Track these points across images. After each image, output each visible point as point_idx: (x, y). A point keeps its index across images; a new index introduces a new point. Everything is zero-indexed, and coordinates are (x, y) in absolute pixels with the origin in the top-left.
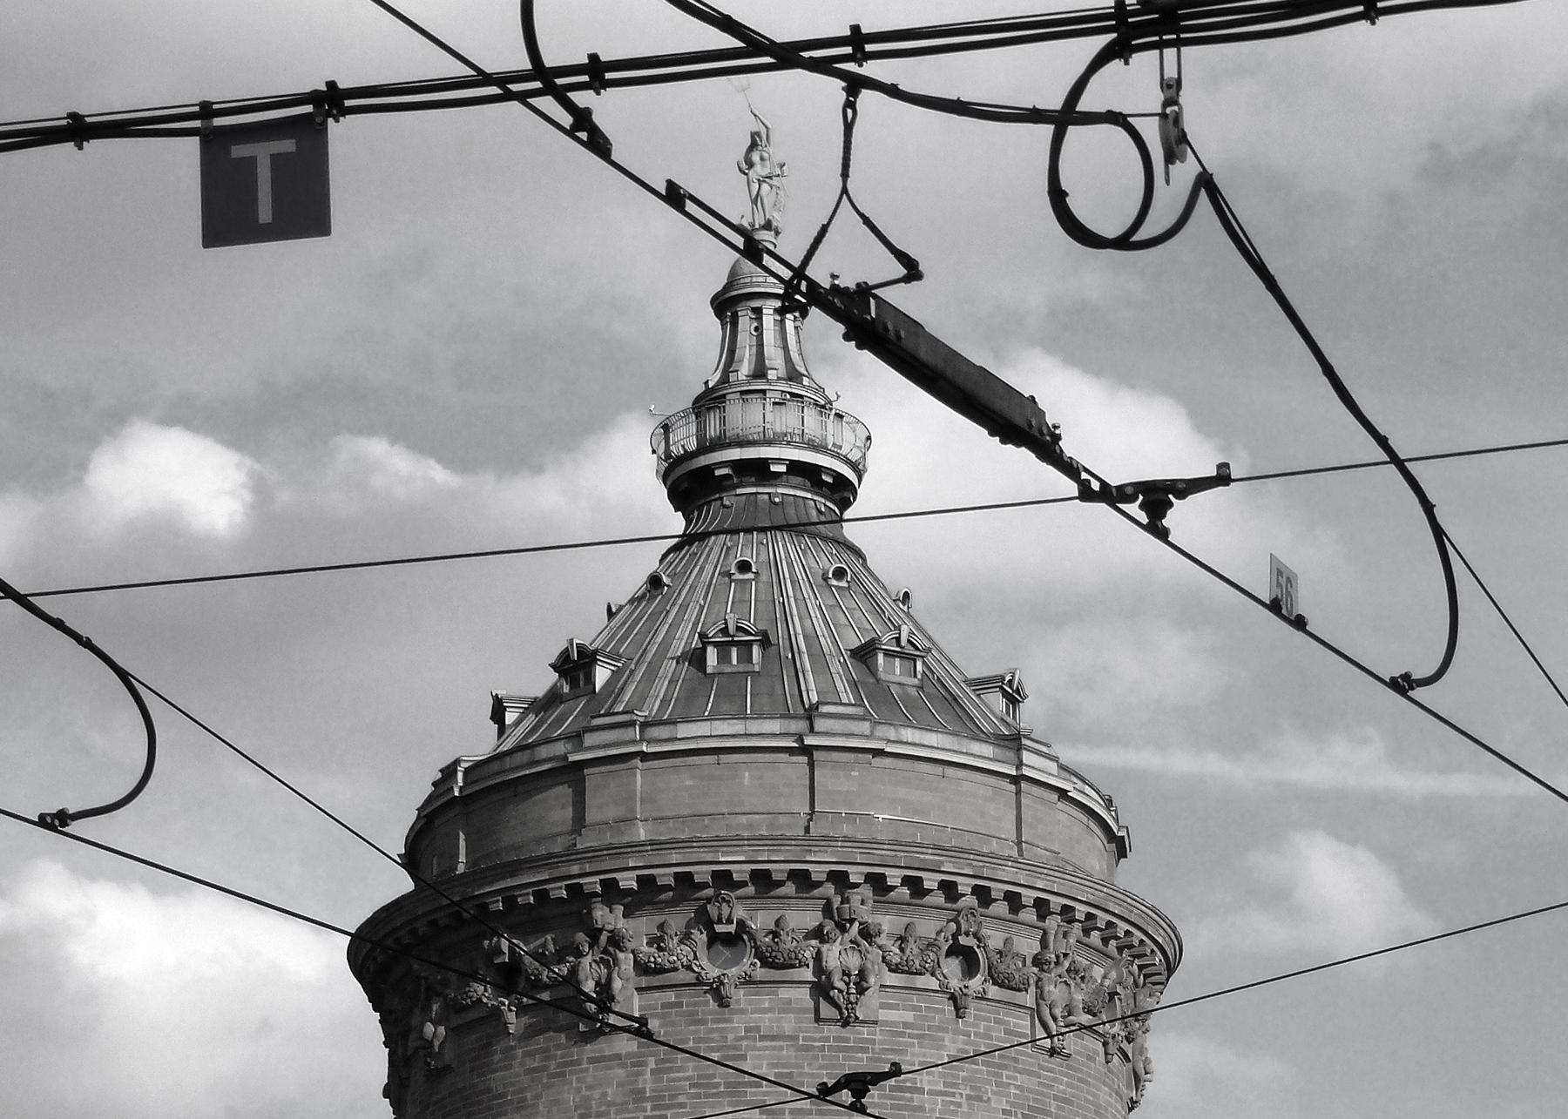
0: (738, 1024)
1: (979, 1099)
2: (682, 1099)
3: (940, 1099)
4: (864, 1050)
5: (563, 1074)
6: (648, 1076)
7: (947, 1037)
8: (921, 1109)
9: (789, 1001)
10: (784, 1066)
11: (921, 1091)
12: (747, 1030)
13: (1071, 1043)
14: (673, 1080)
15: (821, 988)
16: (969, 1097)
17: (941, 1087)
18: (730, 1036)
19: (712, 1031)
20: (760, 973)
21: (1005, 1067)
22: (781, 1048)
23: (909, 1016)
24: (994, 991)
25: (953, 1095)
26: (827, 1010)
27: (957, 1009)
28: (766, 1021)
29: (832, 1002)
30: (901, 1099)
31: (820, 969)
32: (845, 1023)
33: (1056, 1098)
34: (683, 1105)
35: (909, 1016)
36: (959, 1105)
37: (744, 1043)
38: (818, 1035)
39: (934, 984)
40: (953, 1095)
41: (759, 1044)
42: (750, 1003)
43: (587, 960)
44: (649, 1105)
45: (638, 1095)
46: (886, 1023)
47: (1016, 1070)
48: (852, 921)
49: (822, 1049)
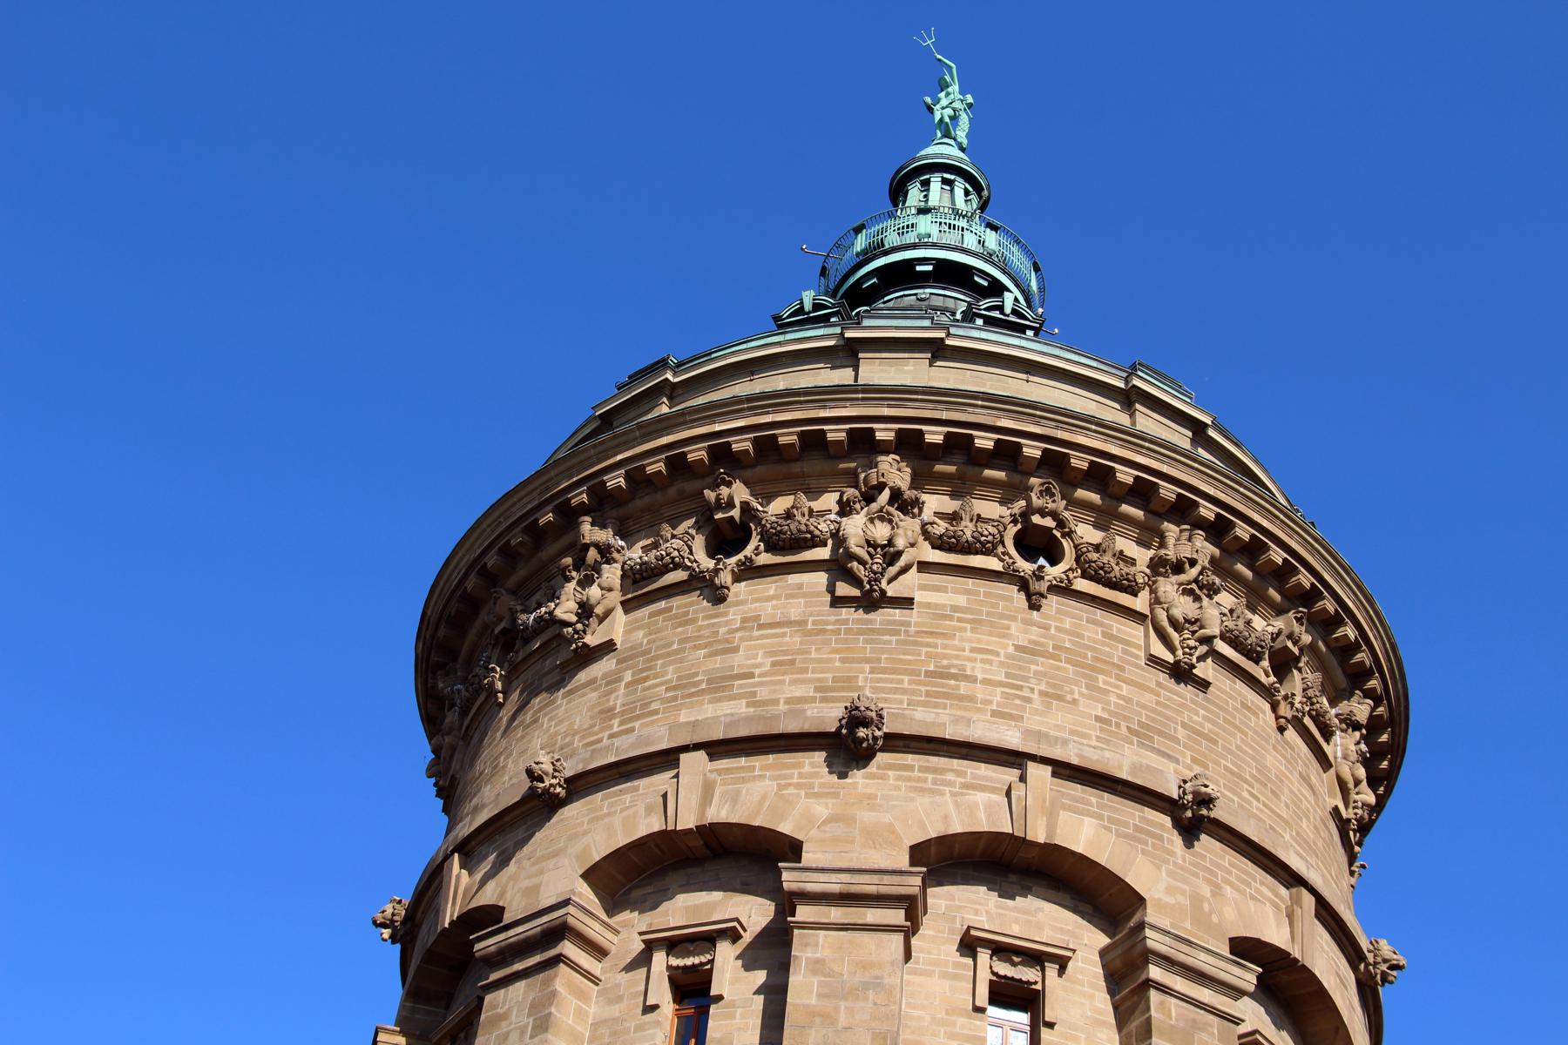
0: (732, 614)
1: (1059, 698)
2: (654, 706)
3: (999, 690)
4: (897, 633)
5: (536, 721)
6: (622, 690)
7: (1014, 628)
8: (971, 698)
9: (800, 586)
10: (785, 653)
11: (973, 679)
12: (744, 620)
13: (1206, 670)
14: (649, 688)
15: (839, 567)
16: (1042, 693)
17: (1002, 678)
18: (722, 630)
19: (700, 628)
20: (765, 558)
21: (1103, 672)
22: (784, 635)
23: (961, 600)
24: (1082, 585)
25: (1020, 688)
26: (843, 589)
27: (1029, 596)
28: (768, 610)
29: (855, 580)
30: (943, 686)
31: (838, 539)
32: (872, 601)
33: (1184, 725)
34: (656, 712)
35: (961, 600)
36: (1029, 700)
37: (738, 635)
38: (833, 618)
39: (993, 564)
40: (1020, 688)
41: (756, 633)
42: (751, 593)
43: (571, 586)
44: (616, 722)
45: (608, 713)
46: (928, 605)
47: (1119, 678)
48: (881, 487)
49: (838, 632)
